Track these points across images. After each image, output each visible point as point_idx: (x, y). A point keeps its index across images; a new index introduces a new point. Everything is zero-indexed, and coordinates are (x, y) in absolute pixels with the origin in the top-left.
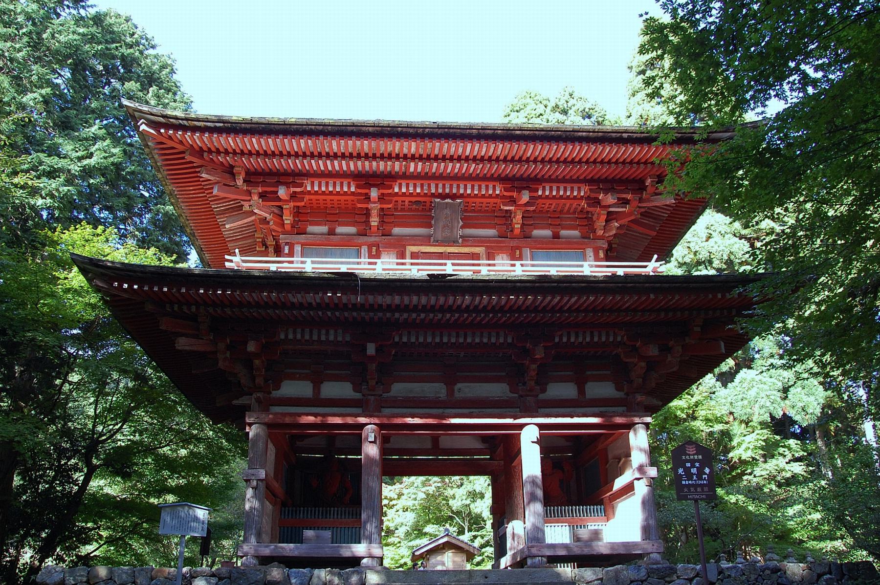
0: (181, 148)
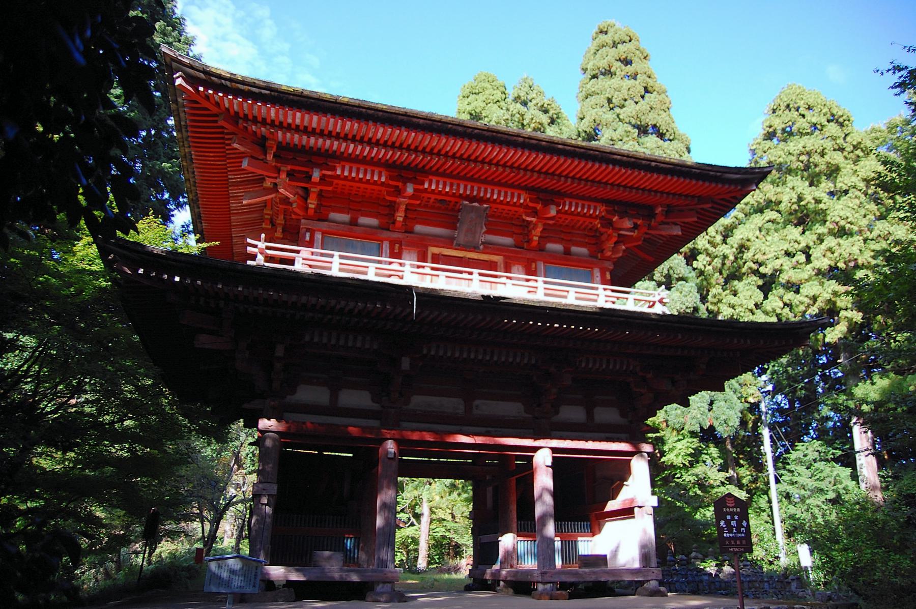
0: (215, 110)
